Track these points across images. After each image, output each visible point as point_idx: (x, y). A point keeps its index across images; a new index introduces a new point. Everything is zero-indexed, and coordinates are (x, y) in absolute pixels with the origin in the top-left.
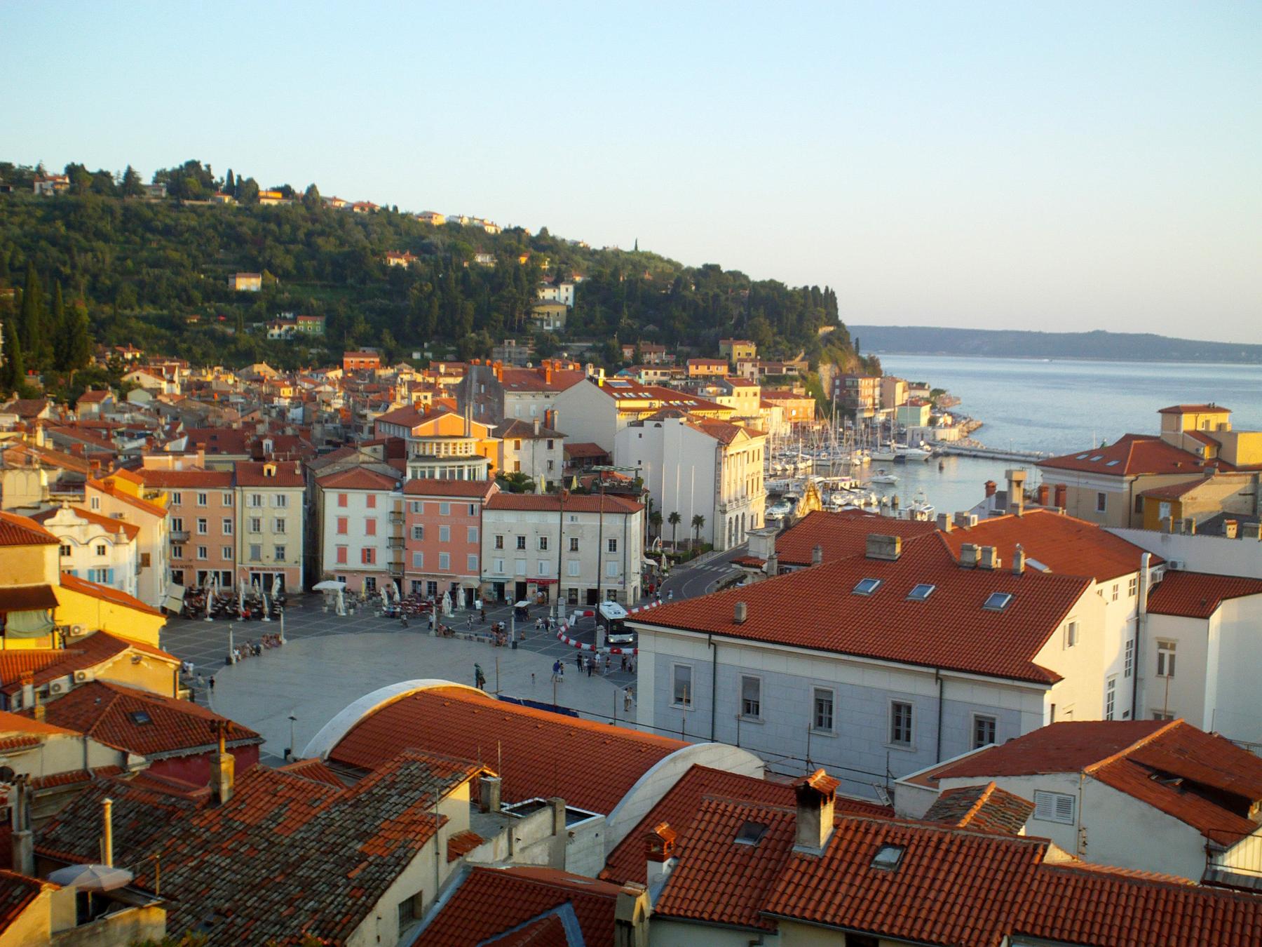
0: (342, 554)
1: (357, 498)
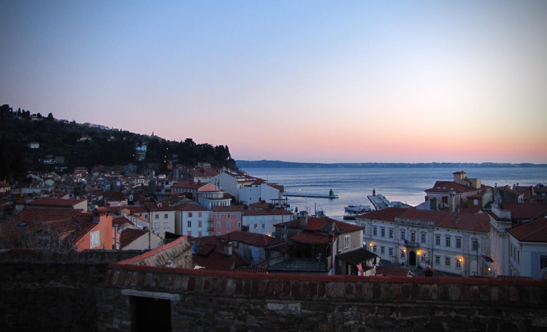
1: (195, 213)
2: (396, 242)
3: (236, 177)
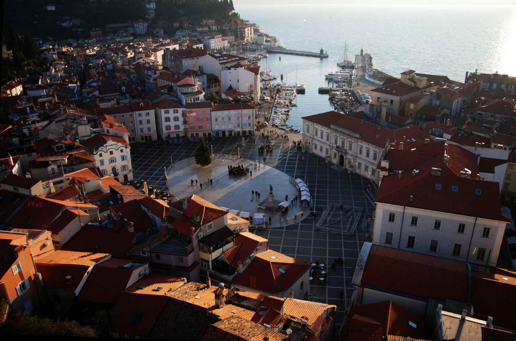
1: (171, 110)
3: (218, 59)
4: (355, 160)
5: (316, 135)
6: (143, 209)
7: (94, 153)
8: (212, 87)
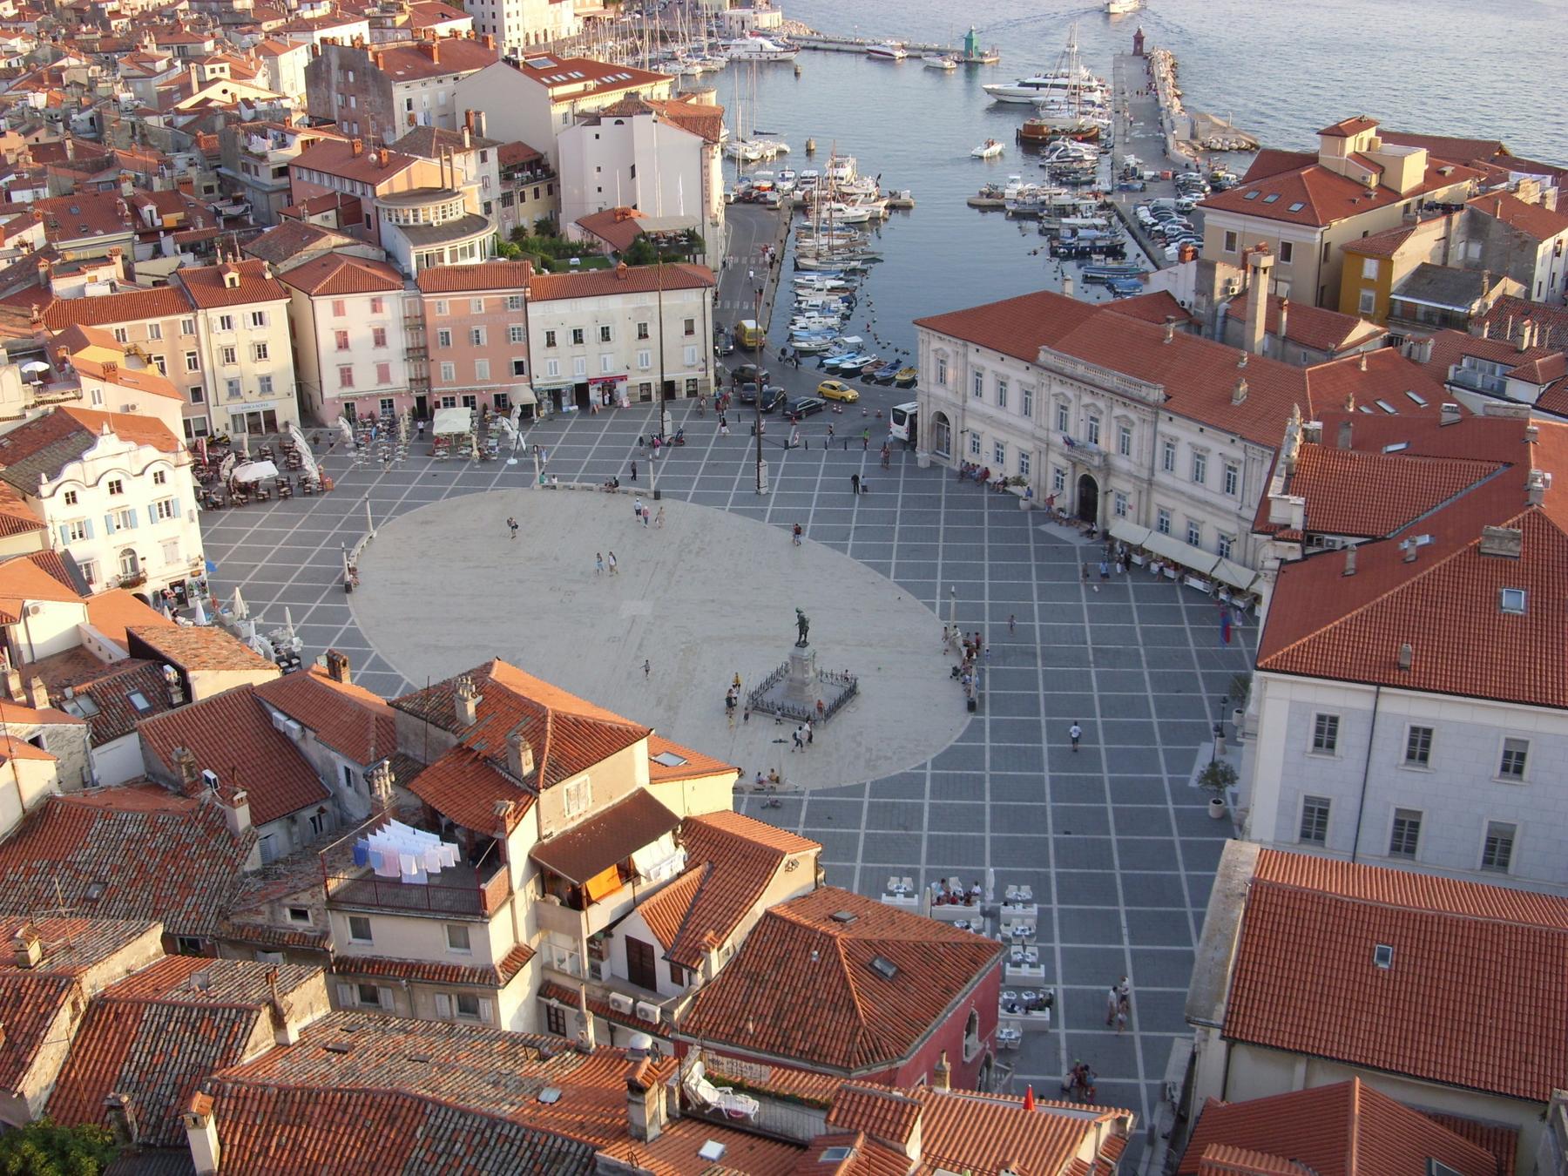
0: (347, 377)
1: (358, 304)
2: (1041, 433)
4: (1144, 498)
5: (978, 392)
6: (282, 728)
7: (45, 489)
8: (523, 200)
